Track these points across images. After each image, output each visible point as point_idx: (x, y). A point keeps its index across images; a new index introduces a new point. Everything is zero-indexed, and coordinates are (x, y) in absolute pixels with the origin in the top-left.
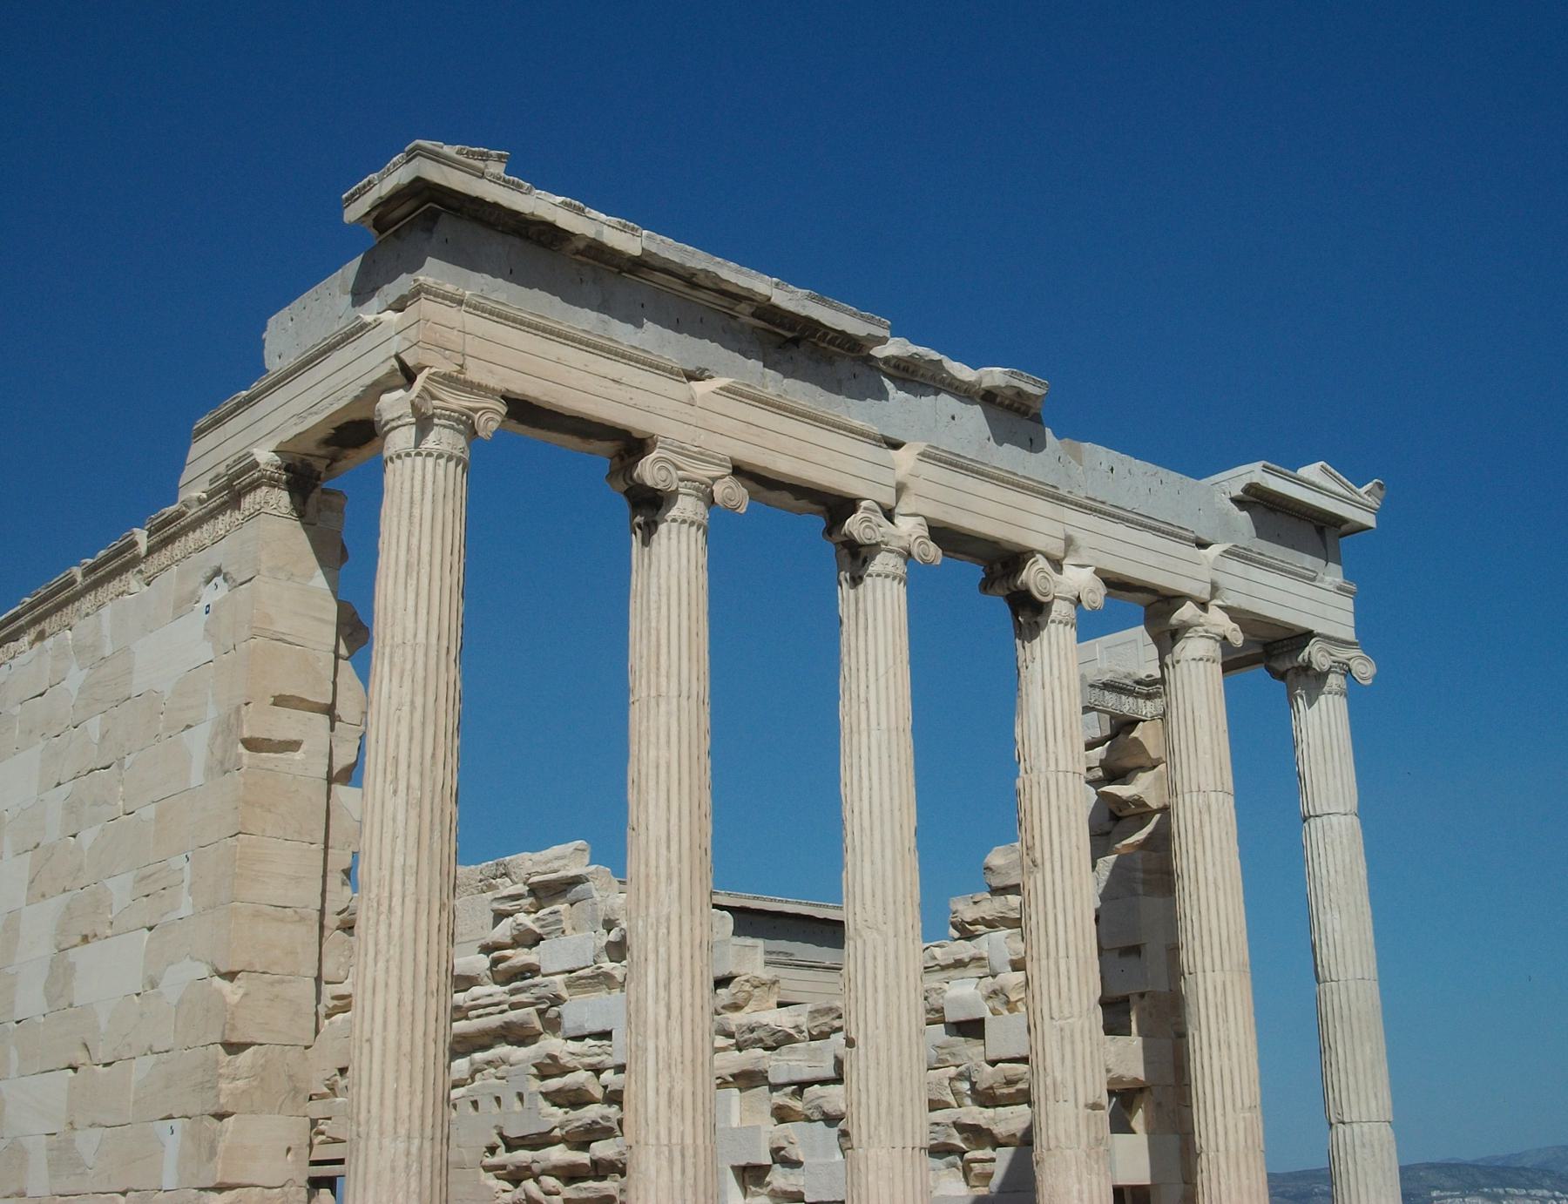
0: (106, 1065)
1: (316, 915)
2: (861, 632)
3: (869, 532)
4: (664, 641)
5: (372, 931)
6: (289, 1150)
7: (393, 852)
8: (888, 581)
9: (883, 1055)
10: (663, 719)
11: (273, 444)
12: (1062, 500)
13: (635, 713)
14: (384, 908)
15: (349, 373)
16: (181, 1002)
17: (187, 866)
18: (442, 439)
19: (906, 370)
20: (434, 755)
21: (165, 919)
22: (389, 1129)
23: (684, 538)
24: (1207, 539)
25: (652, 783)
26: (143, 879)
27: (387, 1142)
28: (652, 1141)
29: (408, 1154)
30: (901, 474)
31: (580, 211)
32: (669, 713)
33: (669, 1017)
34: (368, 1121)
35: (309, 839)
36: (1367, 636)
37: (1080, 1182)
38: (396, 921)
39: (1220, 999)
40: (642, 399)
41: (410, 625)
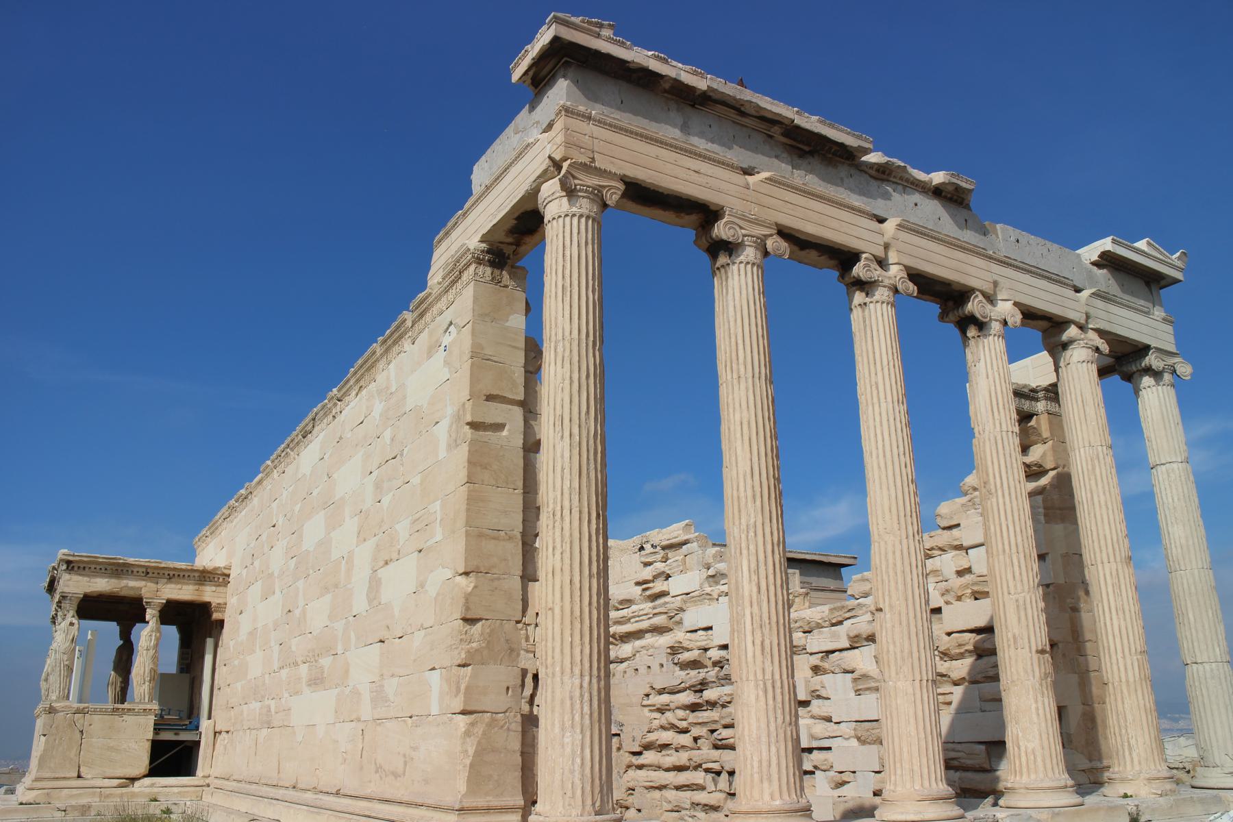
4: (740, 342)
5: (551, 533)
10: (743, 393)
11: (478, 237)
12: (990, 258)
16: (438, 594)
18: (585, 206)
19: (884, 173)
21: (429, 544)
24: (1081, 286)
25: (739, 435)
27: (566, 678)
28: (752, 677)
29: (581, 687)
30: (886, 238)
31: (665, 61)
32: (747, 389)
36: (1185, 348)
37: (1036, 701)
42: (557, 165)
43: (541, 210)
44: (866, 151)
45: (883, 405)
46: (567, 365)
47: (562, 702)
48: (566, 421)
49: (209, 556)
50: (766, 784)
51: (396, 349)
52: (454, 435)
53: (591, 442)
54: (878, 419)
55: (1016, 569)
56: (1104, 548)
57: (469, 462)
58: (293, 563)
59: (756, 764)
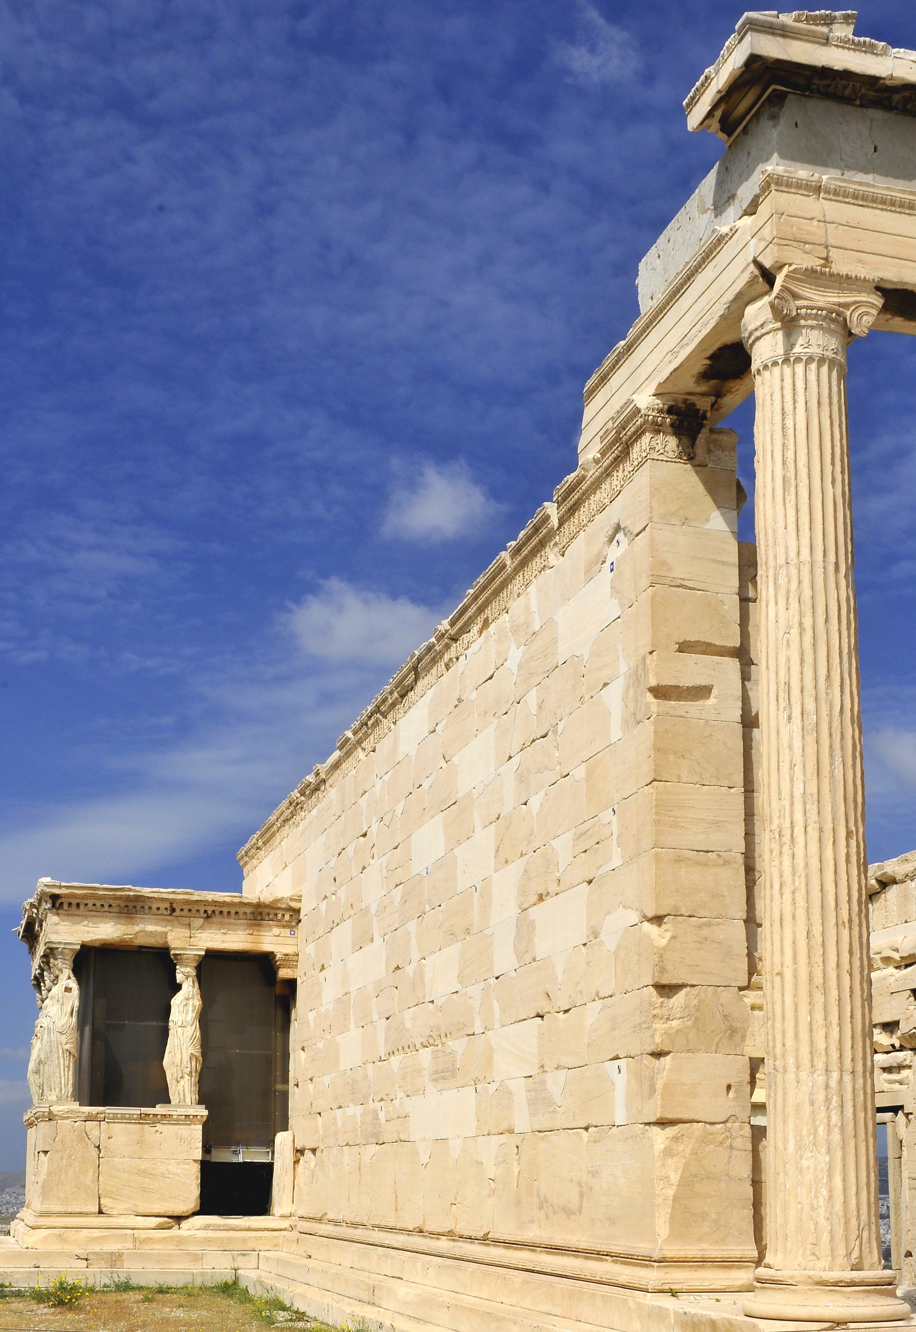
0: (566, 1011)
1: (740, 859)
5: (776, 863)
6: (729, 1087)
7: (792, 781)
15: (712, 294)
16: (618, 948)
17: (614, 819)
20: (828, 676)
21: (601, 871)
22: (806, 1062)
26: (581, 835)
27: (803, 1075)
29: (827, 1087)
34: (783, 1056)
35: (727, 783)
38: (800, 851)
41: (792, 543)
42: (768, 276)
43: (747, 347)
46: (794, 604)
47: (798, 1108)
48: (796, 692)
49: (264, 880)
51: (537, 563)
52: (631, 707)
57: (657, 749)
58: (398, 893)
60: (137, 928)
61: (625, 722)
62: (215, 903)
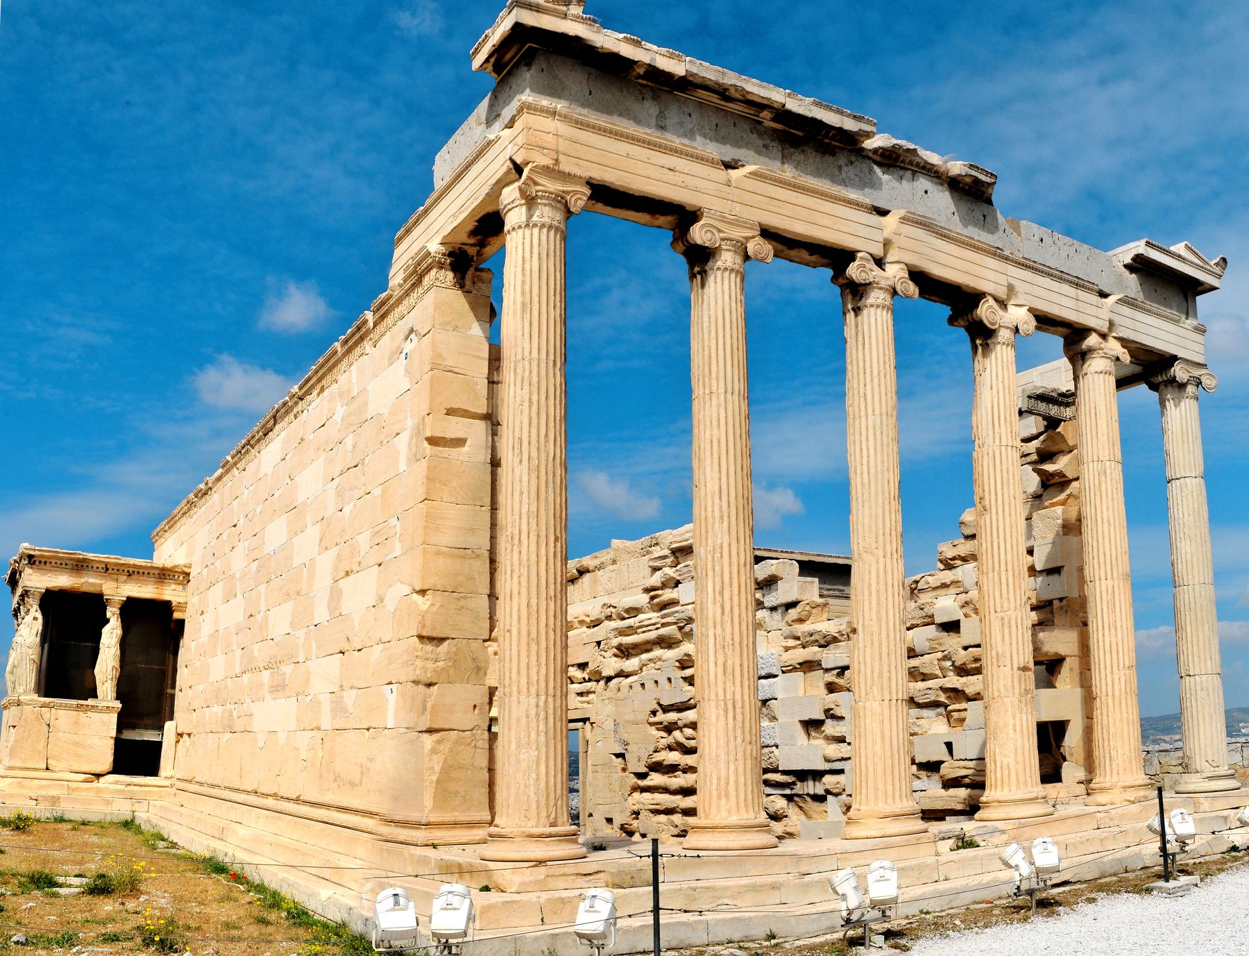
2: (860, 347)
3: (864, 275)
4: (714, 355)
8: (879, 310)
9: (876, 639)
10: (714, 409)
13: (696, 405)
14: (516, 541)
18: (546, 214)
20: (546, 435)
22: (524, 689)
23: (726, 282)
25: (708, 454)
27: (523, 698)
28: (713, 697)
29: (537, 706)
32: (718, 405)
33: (723, 613)
38: (524, 550)
39: (1110, 597)
40: (691, 181)
44: (868, 135)
45: (871, 417)
48: (525, 445)
49: (167, 553)
50: (723, 801)
53: (550, 465)
54: (864, 434)
55: (1004, 586)
56: (1102, 565)
57: (428, 479)
59: (715, 782)
60: (83, 580)
61: (409, 459)
62: (135, 566)
